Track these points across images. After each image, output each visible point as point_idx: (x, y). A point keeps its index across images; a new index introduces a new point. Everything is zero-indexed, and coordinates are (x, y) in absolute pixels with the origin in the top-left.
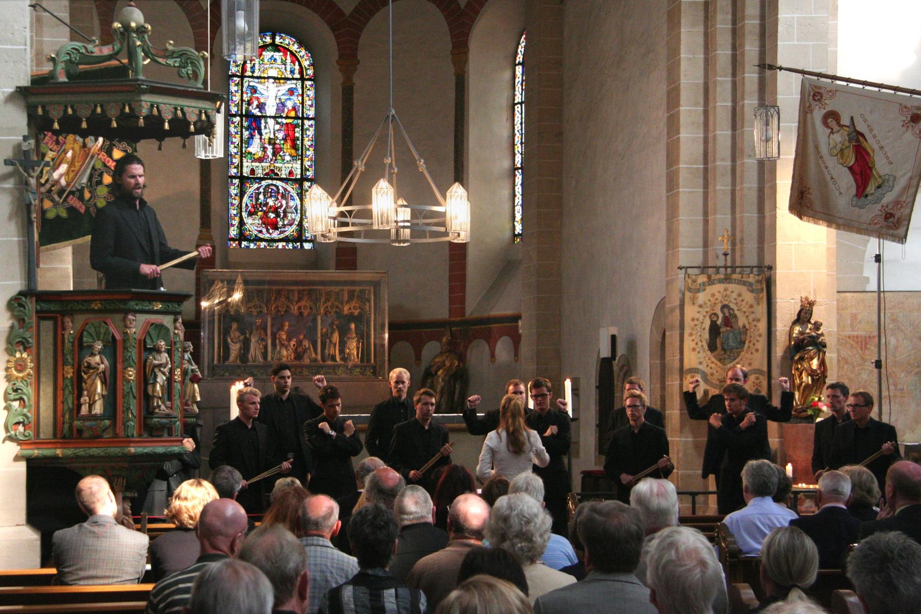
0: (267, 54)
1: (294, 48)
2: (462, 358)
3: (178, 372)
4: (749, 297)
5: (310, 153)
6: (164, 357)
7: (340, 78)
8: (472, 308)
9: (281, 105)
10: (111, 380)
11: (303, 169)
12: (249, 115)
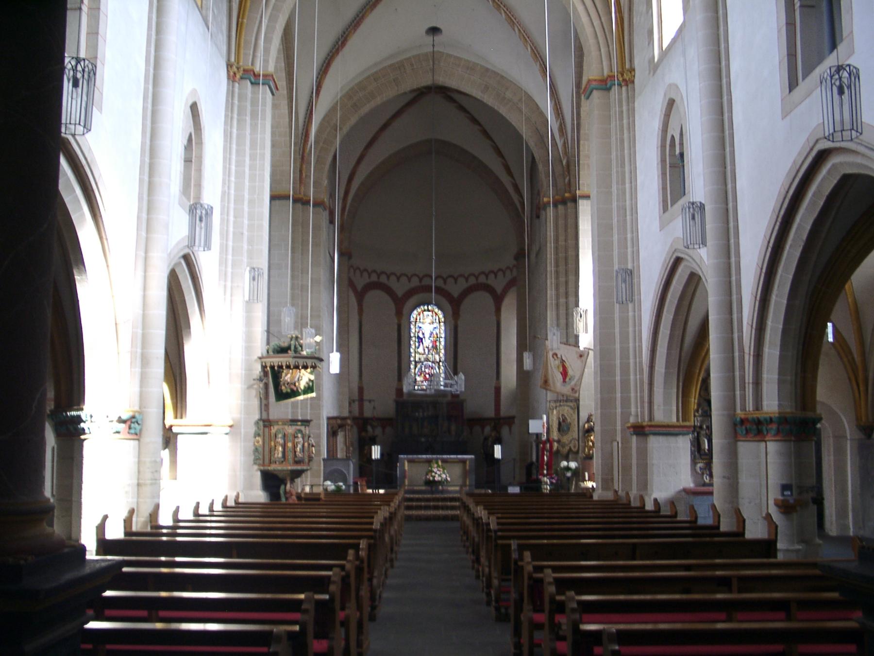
0: (426, 313)
1: (436, 310)
2: (499, 432)
3: (306, 444)
4: (571, 411)
5: (443, 351)
6: (301, 440)
7: (453, 322)
8: (504, 412)
9: (432, 333)
10: (284, 446)
11: (440, 358)
12: (418, 337)
